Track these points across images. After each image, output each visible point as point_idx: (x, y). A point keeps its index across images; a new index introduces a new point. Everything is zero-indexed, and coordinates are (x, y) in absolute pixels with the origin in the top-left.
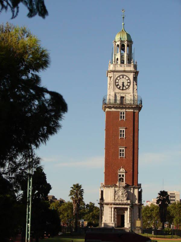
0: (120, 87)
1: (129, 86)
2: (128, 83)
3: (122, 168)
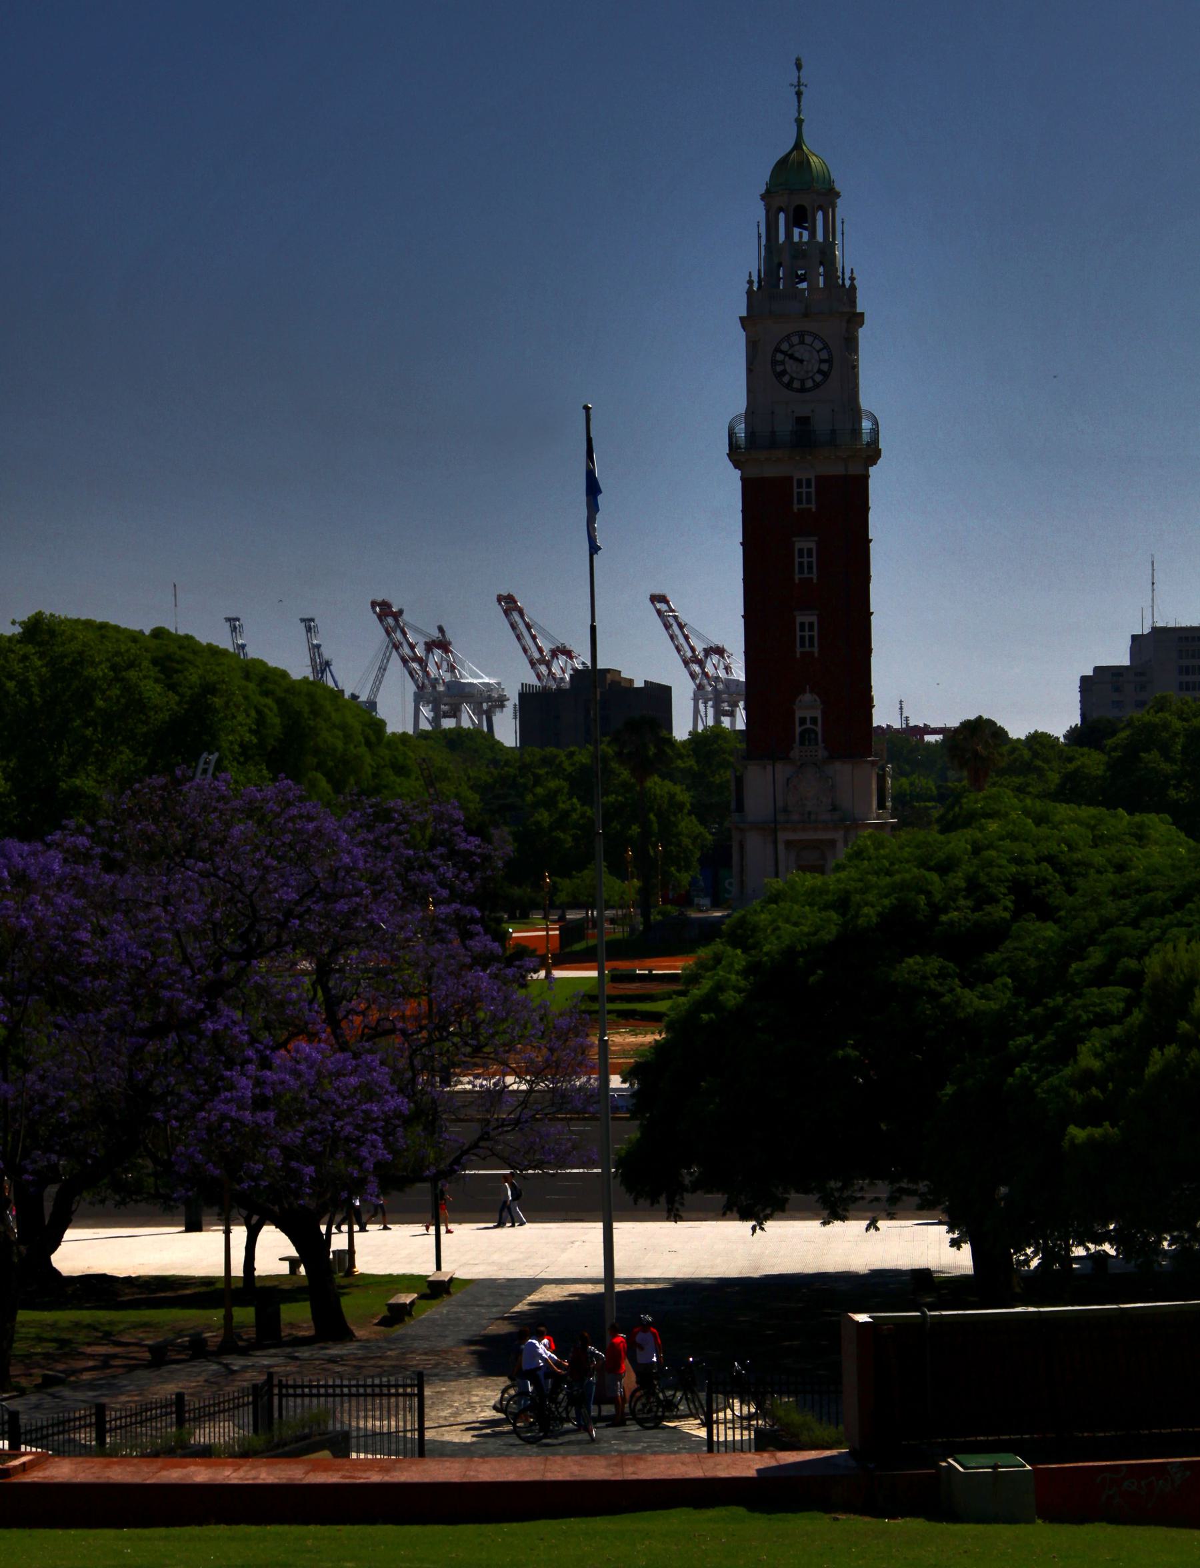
0: (792, 380)
1: (826, 375)
2: (822, 361)
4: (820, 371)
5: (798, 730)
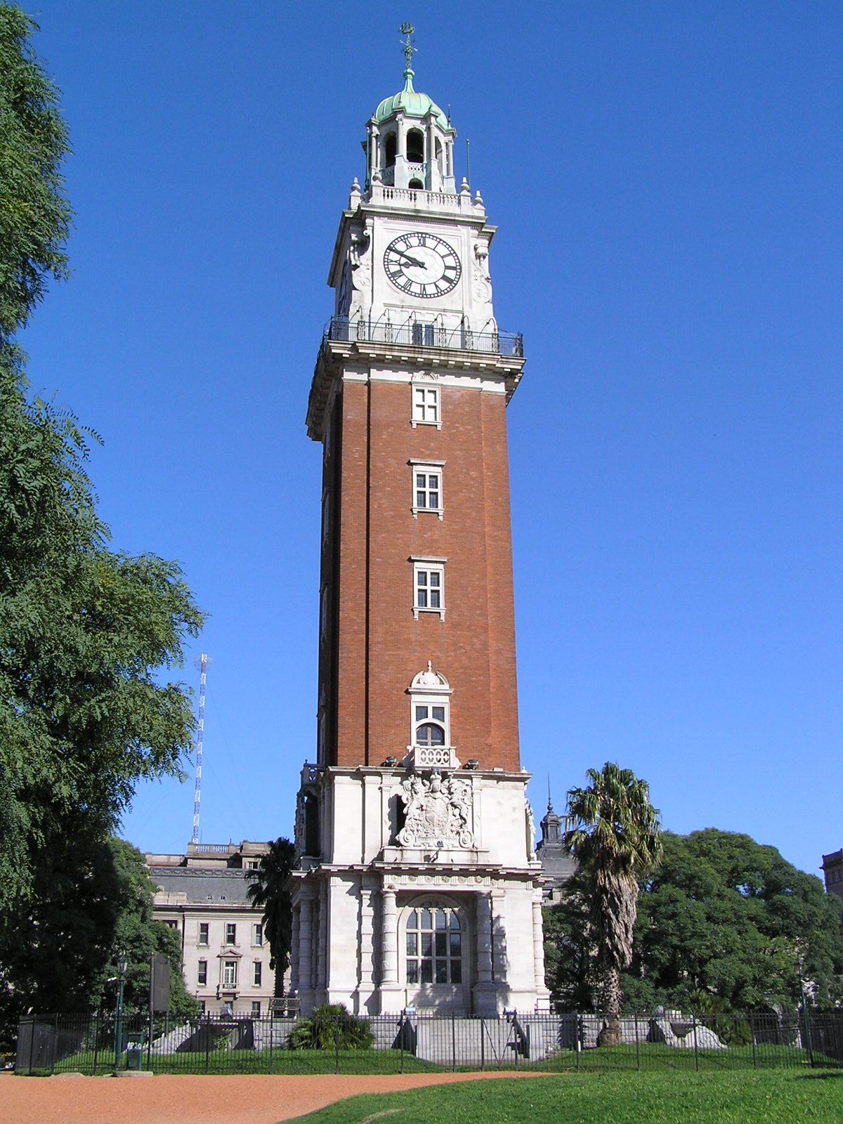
2: (447, 268)
3: (433, 671)
4: (444, 278)
5: (415, 725)
